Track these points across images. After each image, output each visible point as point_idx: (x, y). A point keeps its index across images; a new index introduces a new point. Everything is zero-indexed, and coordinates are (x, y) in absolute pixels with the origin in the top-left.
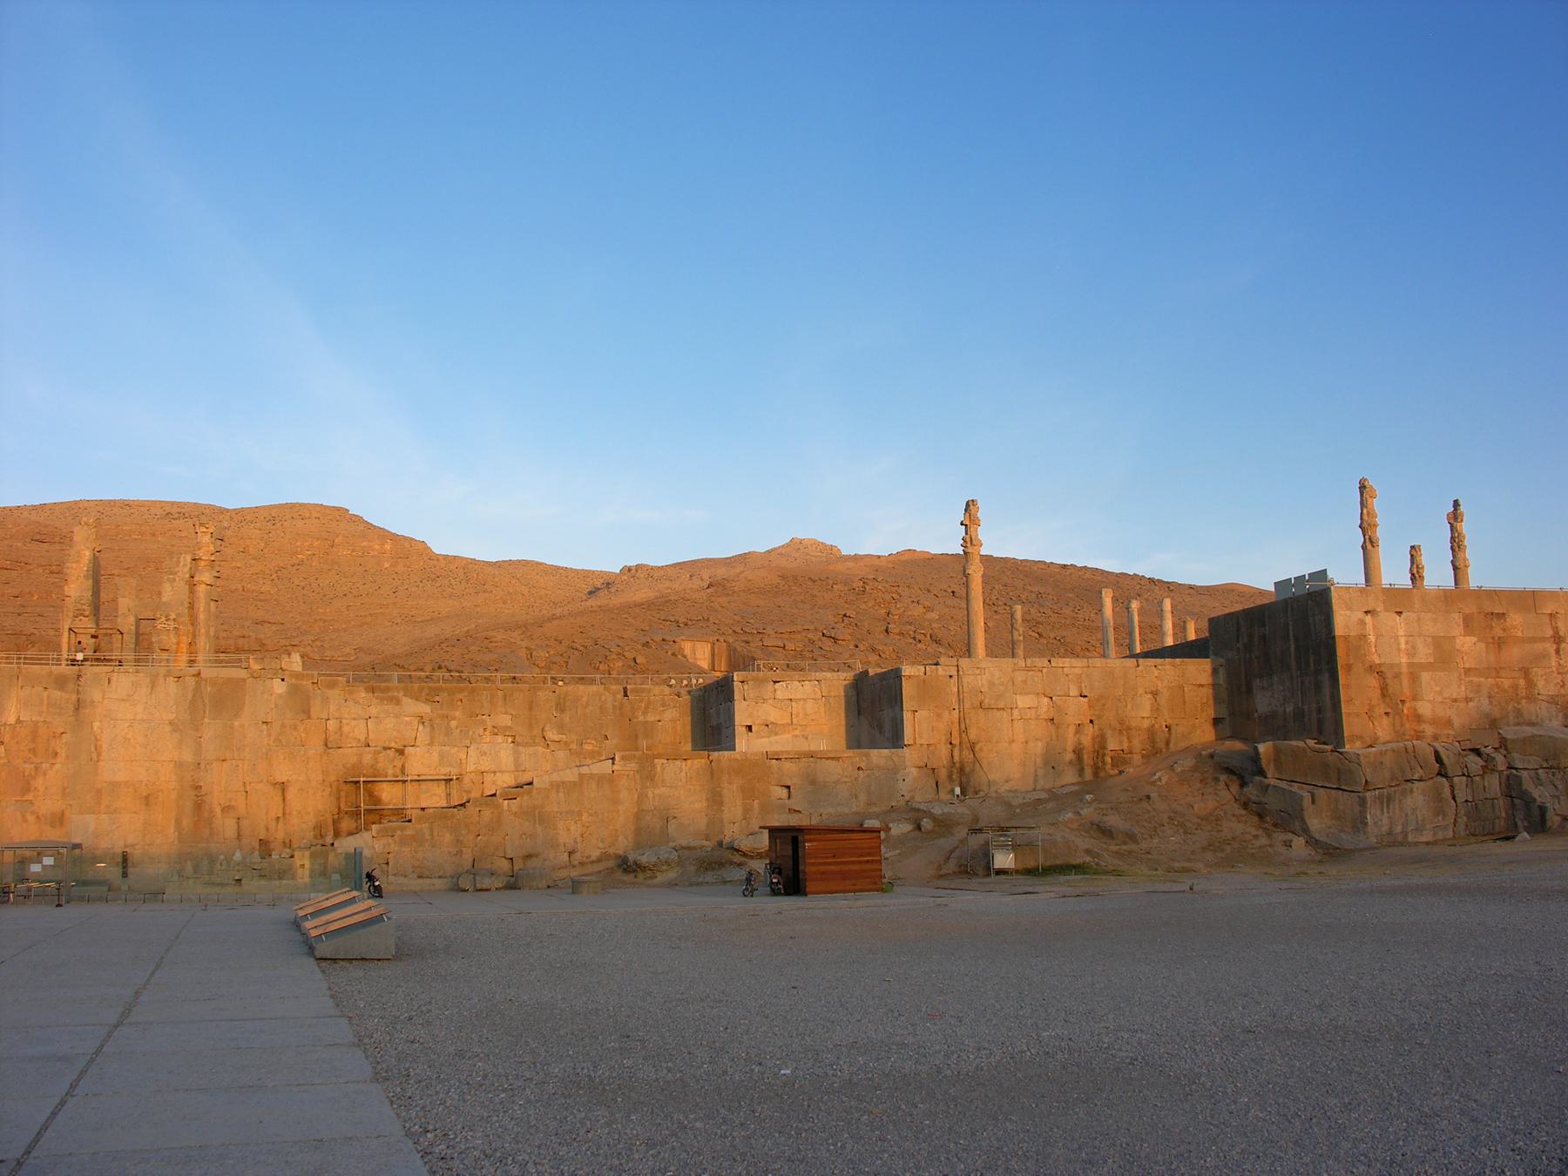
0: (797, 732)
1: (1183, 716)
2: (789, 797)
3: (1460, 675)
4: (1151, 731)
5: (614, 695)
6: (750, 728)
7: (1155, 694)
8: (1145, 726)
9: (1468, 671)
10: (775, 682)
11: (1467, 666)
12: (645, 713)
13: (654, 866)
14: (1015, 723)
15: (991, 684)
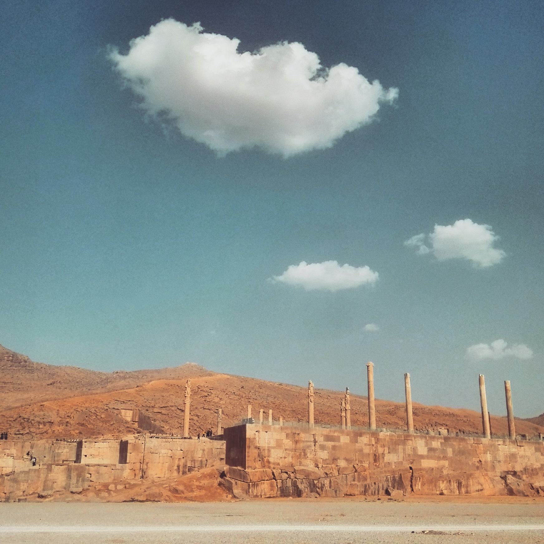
0: (100, 458)
1: (211, 457)
2: (91, 477)
3: (284, 450)
4: (201, 461)
5: (49, 444)
6: (86, 456)
7: (204, 450)
8: (200, 460)
9: (286, 450)
10: (95, 442)
11: (286, 448)
12: (59, 449)
13: (46, 496)
14: (160, 457)
15: (154, 446)
